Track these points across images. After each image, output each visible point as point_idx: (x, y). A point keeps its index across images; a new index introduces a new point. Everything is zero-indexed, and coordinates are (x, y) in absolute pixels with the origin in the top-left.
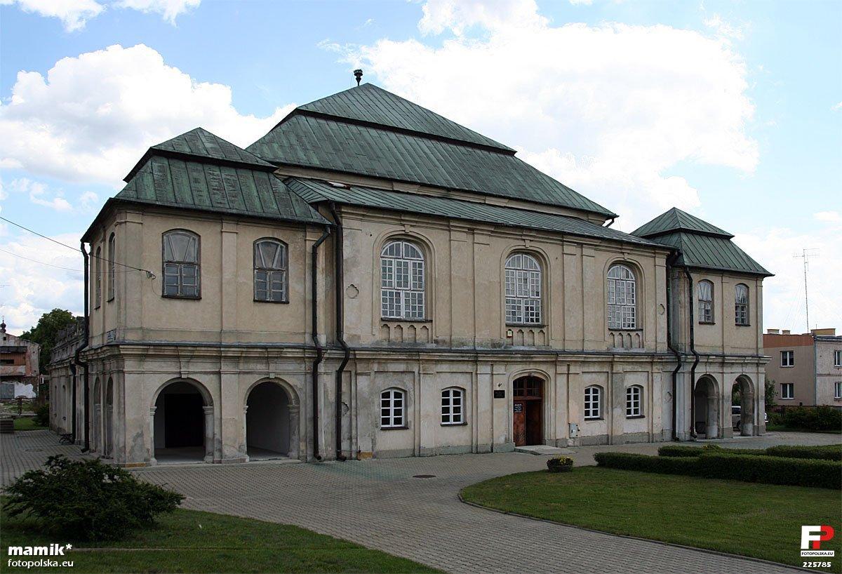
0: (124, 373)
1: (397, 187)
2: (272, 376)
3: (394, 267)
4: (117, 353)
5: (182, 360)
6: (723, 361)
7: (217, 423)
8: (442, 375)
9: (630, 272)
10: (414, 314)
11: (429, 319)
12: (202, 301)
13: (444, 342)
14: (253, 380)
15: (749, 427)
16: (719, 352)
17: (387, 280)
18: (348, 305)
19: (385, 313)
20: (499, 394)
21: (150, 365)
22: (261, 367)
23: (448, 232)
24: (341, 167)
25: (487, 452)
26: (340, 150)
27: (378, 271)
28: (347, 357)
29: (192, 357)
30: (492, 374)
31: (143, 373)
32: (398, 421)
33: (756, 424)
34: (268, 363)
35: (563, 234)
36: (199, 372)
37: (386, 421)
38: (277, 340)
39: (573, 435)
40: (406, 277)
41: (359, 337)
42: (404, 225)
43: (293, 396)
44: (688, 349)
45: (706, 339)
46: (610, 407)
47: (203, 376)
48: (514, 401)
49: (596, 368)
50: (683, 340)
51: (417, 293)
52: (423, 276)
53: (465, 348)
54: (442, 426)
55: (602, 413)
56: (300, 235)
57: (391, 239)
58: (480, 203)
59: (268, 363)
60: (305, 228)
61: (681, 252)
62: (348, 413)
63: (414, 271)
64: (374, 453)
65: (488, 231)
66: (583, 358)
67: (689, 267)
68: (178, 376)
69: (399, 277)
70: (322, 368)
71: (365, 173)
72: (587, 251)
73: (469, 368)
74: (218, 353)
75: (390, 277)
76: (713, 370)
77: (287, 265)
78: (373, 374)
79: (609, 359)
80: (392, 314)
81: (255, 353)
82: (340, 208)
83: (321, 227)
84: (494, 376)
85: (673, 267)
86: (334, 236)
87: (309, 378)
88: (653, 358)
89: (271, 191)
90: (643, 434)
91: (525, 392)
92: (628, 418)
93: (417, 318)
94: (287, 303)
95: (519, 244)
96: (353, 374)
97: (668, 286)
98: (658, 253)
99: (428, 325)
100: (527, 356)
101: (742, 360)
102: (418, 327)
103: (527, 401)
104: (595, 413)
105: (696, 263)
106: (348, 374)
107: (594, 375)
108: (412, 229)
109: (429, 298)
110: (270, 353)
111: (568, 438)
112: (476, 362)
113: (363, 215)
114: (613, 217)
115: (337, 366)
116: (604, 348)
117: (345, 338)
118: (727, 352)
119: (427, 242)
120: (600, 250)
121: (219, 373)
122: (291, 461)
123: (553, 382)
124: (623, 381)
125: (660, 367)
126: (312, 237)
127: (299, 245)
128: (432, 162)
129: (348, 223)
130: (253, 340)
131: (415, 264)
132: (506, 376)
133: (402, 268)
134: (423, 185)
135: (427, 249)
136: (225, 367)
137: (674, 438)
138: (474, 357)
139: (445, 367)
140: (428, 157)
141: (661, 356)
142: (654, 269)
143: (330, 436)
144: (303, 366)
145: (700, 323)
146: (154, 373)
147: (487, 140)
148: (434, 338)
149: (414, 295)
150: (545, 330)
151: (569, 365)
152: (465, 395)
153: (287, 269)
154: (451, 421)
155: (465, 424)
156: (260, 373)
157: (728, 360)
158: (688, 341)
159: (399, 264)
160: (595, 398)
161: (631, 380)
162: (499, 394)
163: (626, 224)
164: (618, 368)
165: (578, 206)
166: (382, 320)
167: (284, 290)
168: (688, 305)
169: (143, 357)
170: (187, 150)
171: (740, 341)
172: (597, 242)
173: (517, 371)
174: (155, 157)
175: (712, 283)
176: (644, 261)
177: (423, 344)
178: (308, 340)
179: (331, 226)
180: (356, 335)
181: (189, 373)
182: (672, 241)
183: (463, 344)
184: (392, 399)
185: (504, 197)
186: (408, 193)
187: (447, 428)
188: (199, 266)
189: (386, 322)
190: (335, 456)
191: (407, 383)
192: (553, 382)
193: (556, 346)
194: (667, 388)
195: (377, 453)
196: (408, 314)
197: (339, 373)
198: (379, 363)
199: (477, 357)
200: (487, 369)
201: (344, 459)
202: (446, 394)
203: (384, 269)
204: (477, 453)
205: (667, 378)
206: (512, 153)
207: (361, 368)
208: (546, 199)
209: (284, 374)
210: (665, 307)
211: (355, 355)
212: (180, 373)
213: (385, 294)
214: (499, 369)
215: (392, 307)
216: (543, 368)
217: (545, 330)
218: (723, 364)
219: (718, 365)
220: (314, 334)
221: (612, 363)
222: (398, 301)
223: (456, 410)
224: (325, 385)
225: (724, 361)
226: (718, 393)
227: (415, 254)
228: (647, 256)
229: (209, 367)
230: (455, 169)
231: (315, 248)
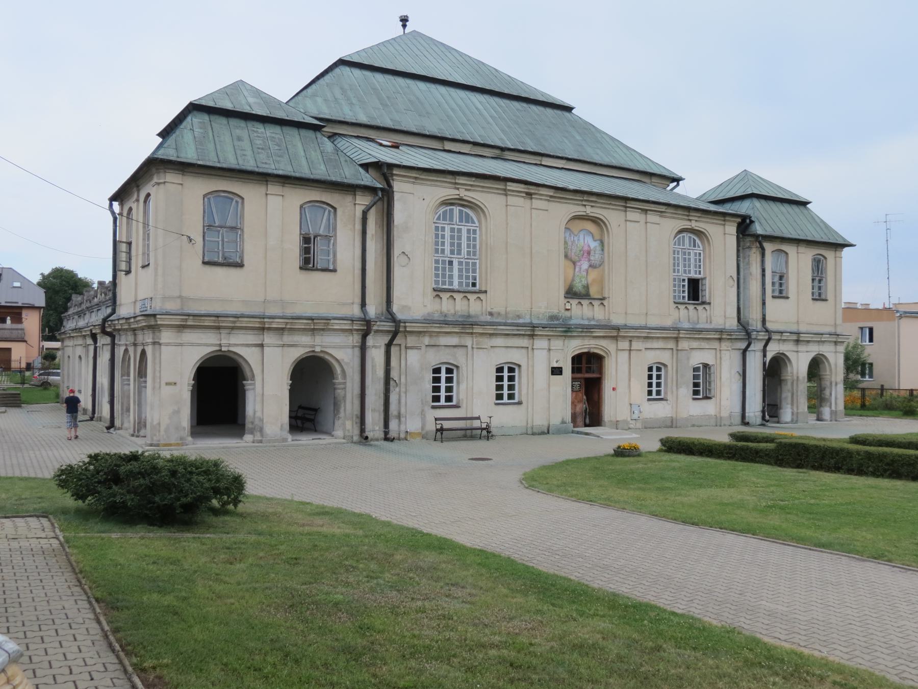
0: (160, 344)
1: (448, 146)
2: (318, 349)
3: (447, 233)
4: (153, 323)
5: (222, 331)
6: (798, 339)
7: (258, 399)
8: (497, 350)
9: (698, 241)
10: (467, 285)
11: (483, 289)
12: (245, 268)
13: (499, 314)
14: (297, 354)
15: (826, 412)
16: (794, 328)
17: (440, 247)
19: (437, 282)
20: (556, 371)
21: (189, 336)
22: (305, 339)
23: (504, 197)
24: (389, 124)
25: (543, 433)
26: (387, 105)
27: (431, 238)
28: (397, 330)
29: (233, 328)
30: (550, 350)
31: (181, 345)
32: (449, 399)
33: (833, 408)
34: (313, 335)
35: (626, 199)
36: (240, 344)
37: (436, 399)
38: (323, 311)
39: (635, 416)
40: (459, 245)
41: (410, 308)
42: (458, 189)
43: (338, 370)
44: (759, 326)
45: (780, 314)
46: (675, 388)
47: (247, 349)
48: (573, 378)
50: (753, 317)
51: (471, 261)
52: (478, 242)
53: (521, 321)
54: (496, 404)
55: (666, 393)
56: (349, 198)
57: (446, 203)
58: (536, 164)
59: (313, 335)
60: (355, 192)
61: (753, 219)
62: (397, 389)
63: (469, 239)
64: (424, 432)
65: (547, 196)
66: (647, 333)
67: (762, 236)
68: (217, 348)
69: (452, 244)
70: (370, 341)
71: (414, 130)
72: (652, 218)
73: (525, 342)
74: (262, 325)
75: (443, 244)
76: (786, 348)
77: (335, 229)
78: (423, 348)
79: (675, 334)
80: (444, 283)
81: (300, 324)
82: (392, 170)
83: (371, 190)
84: (551, 352)
85: (744, 235)
86: (384, 198)
87: (357, 352)
88: (722, 335)
89: (318, 151)
90: (709, 416)
91: (584, 370)
92: (694, 399)
93: (471, 288)
94: (335, 271)
95: (579, 210)
96: (403, 347)
97: (738, 256)
98: (729, 221)
99: (482, 296)
100: (587, 330)
101: (819, 337)
102: (472, 297)
103: (586, 380)
104: (658, 393)
105: (769, 232)
106: (397, 348)
107: (658, 352)
108: (467, 193)
109: (483, 267)
110: (317, 325)
111: (629, 419)
112: (532, 336)
113: (416, 178)
114: (677, 180)
115: (386, 339)
116: (668, 323)
117: (395, 308)
118: (802, 329)
119: (482, 206)
120: (665, 217)
121: (262, 346)
122: (337, 441)
123: (614, 359)
124: (688, 359)
126: (363, 200)
127: (349, 209)
128: (485, 119)
129: (399, 186)
130: (298, 311)
131: (469, 231)
132: (564, 352)
133: (456, 235)
134: (476, 144)
135: (482, 215)
136: (269, 338)
137: (744, 422)
138: (531, 331)
139: (499, 341)
140: (481, 114)
141: (729, 333)
142: (724, 237)
143: (377, 414)
144: (351, 338)
145: (773, 297)
146: (192, 345)
147: (543, 94)
148: (489, 310)
149: (467, 264)
150: (605, 302)
151: (631, 341)
152: (520, 372)
153: (335, 235)
154: (505, 400)
155: (520, 403)
156: (304, 346)
157: (803, 337)
158: (759, 316)
159: (452, 230)
160: (659, 377)
161: (698, 358)
162: (556, 371)
163: (695, 187)
164: (684, 345)
165: (641, 168)
166: (434, 290)
167: (331, 256)
168: (759, 276)
169: (181, 328)
170: (228, 105)
171: (818, 317)
172: (663, 208)
173: (577, 346)
174: (195, 112)
175: (787, 254)
176: (712, 228)
177: (476, 316)
178: (356, 311)
179: (382, 190)
180: (406, 306)
181: (230, 345)
182: (743, 208)
183: (519, 317)
184: (443, 375)
185: (562, 158)
186: (460, 153)
187: (501, 407)
188: (242, 230)
189: (438, 292)
190: (382, 436)
191: (459, 358)
192: (614, 359)
193: (617, 320)
194: (738, 367)
195: (427, 433)
196: (460, 284)
197: (389, 346)
198: (431, 336)
199: (533, 331)
201: (393, 440)
202: (500, 370)
203: (437, 236)
204: (533, 434)
205: (737, 356)
206: (569, 109)
207: (411, 340)
208: (606, 160)
209: (330, 347)
210: (735, 279)
211: (405, 327)
212: (220, 345)
213: (437, 262)
214: (557, 343)
215: (444, 276)
216: (604, 343)
217: (605, 302)
218: (797, 341)
219: (792, 343)
220: (363, 304)
221: (677, 339)
222: (451, 270)
223: (511, 388)
224: (373, 359)
225: (798, 339)
226: (792, 373)
227: (468, 219)
229: (251, 338)
230: (509, 127)
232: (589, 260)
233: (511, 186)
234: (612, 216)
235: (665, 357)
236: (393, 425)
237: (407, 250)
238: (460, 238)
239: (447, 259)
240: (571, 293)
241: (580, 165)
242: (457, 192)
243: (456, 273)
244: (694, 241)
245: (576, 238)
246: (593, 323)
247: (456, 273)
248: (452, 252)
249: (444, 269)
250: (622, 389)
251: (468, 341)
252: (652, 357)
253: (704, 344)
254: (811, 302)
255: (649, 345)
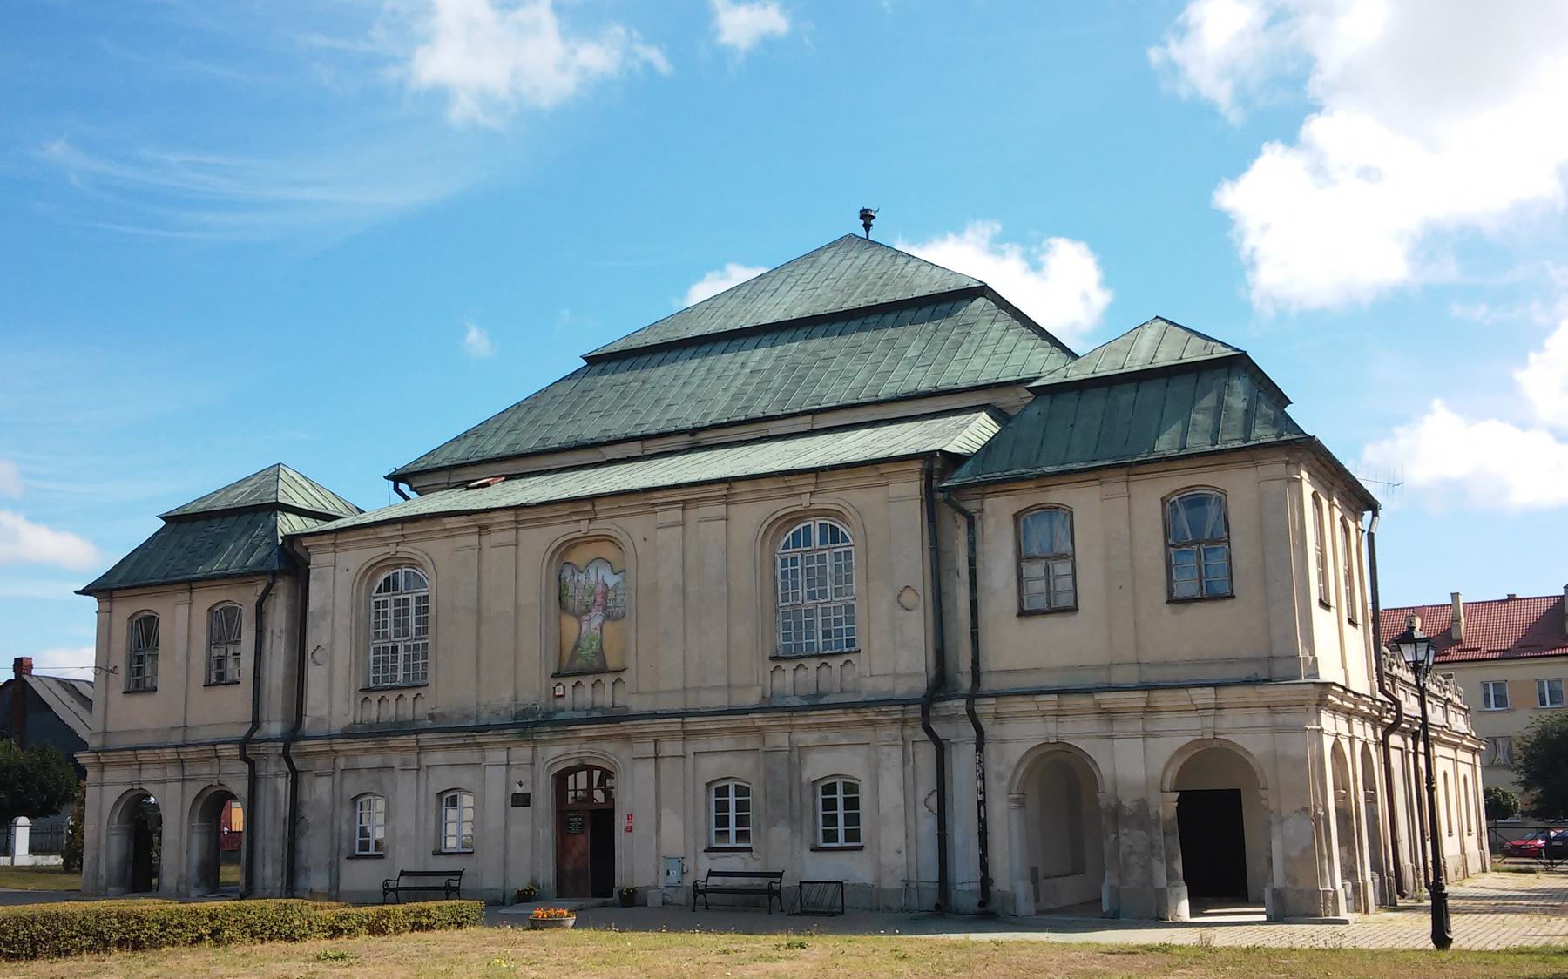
13: (443, 716)
18: (314, 674)
19: (376, 680)
20: (521, 800)
40: (406, 622)
49: (727, 743)
57: (376, 567)
69: (397, 623)
75: (385, 625)
76: (1080, 730)
80: (385, 679)
107: (727, 758)
116: (752, 698)
125: (895, 731)
139: (437, 757)
161: (819, 766)
162: (521, 800)
193: (637, 704)
200: (499, 755)
203: (377, 617)
213: (377, 651)
214: (523, 753)
216: (609, 747)
217: (623, 676)
228: (862, 487)
231: (259, 605)
232: (605, 608)
233: (452, 522)
234: (633, 527)
235: (741, 768)
236: (302, 882)
237: (325, 640)
238: (406, 612)
239: (390, 645)
240: (566, 670)
241: (845, 413)
242: (387, 549)
243: (401, 663)
244: (834, 530)
245: (582, 577)
246: (595, 714)
247: (401, 663)
248: (397, 634)
249: (385, 660)
250: (643, 827)
251: (396, 760)
252: (712, 768)
253: (832, 736)
254: (1166, 609)
255: (701, 746)
